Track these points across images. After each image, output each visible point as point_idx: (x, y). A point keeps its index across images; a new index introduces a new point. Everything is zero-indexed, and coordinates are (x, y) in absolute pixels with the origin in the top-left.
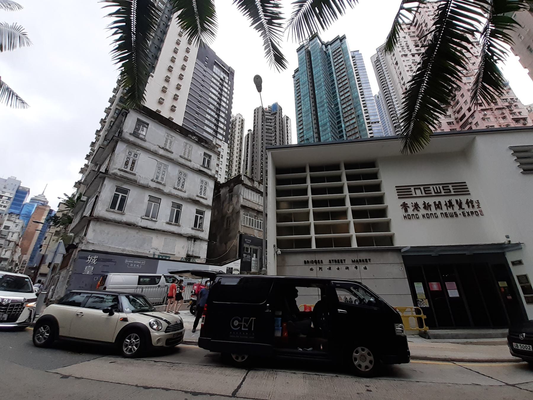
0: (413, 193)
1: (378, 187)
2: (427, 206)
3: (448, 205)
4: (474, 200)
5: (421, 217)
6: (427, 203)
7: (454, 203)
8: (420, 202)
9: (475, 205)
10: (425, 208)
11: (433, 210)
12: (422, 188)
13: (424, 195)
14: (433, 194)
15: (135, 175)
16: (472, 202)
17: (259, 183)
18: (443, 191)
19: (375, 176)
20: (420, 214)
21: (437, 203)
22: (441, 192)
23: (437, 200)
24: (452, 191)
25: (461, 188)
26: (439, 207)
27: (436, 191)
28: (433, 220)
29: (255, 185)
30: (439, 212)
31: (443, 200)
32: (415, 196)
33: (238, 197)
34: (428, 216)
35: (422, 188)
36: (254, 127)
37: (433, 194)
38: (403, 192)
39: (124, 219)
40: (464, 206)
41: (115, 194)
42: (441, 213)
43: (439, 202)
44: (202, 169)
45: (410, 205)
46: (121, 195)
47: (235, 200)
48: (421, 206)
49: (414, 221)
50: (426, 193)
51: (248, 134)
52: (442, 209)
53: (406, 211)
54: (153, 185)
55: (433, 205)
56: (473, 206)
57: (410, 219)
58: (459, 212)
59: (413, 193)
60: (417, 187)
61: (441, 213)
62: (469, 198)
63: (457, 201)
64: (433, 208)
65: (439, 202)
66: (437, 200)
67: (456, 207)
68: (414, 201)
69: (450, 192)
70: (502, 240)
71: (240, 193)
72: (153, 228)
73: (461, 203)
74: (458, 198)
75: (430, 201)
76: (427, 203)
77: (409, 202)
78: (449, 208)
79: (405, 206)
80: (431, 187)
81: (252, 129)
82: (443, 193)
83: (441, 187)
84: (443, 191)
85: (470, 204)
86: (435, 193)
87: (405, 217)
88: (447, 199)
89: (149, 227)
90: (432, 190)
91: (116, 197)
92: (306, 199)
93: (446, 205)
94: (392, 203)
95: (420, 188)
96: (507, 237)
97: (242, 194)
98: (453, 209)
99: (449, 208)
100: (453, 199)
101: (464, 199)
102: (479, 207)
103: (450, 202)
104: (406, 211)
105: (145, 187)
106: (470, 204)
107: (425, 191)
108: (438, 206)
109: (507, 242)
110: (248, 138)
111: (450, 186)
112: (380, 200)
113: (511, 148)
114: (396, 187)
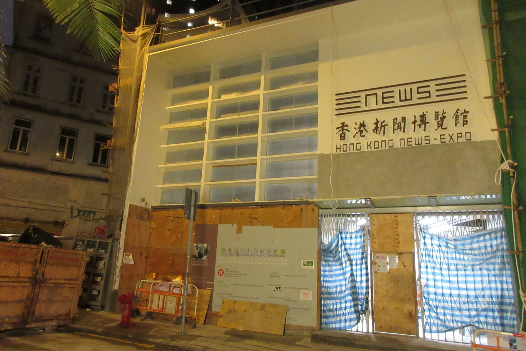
3: (418, 122)
6: (381, 120)
7: (430, 118)
8: (370, 120)
10: (376, 130)
12: (379, 92)
14: (398, 103)
15: (38, 98)
19: (314, 77)
21: (399, 120)
22: (411, 99)
23: (399, 114)
24: (434, 93)
26: (399, 127)
27: (403, 98)
31: (411, 113)
32: (366, 109)
37: (398, 103)
38: (346, 102)
39: (29, 161)
40: (449, 122)
41: (14, 128)
43: (404, 119)
44: (22, 98)
46: (22, 129)
48: (371, 126)
50: (383, 103)
52: (404, 131)
53: (343, 137)
54: (66, 109)
55: (391, 124)
56: (465, 123)
60: (370, 92)
62: (462, 105)
63: (437, 114)
65: (404, 119)
66: (399, 114)
68: (359, 118)
72: (69, 173)
73: (443, 118)
74: (439, 108)
75: (387, 117)
76: (381, 120)
78: (417, 127)
80: (396, 89)
82: (415, 101)
83: (414, 87)
84: (415, 96)
85: (461, 119)
86: (401, 101)
88: (418, 111)
89: (63, 172)
90: (397, 96)
91: (16, 134)
92: (253, 120)
93: (414, 122)
95: (376, 94)
98: (425, 130)
99: (417, 127)
100: (430, 110)
101: (450, 108)
103: (423, 117)
104: (343, 137)
105: (57, 114)
106: (461, 119)
112: (312, 120)
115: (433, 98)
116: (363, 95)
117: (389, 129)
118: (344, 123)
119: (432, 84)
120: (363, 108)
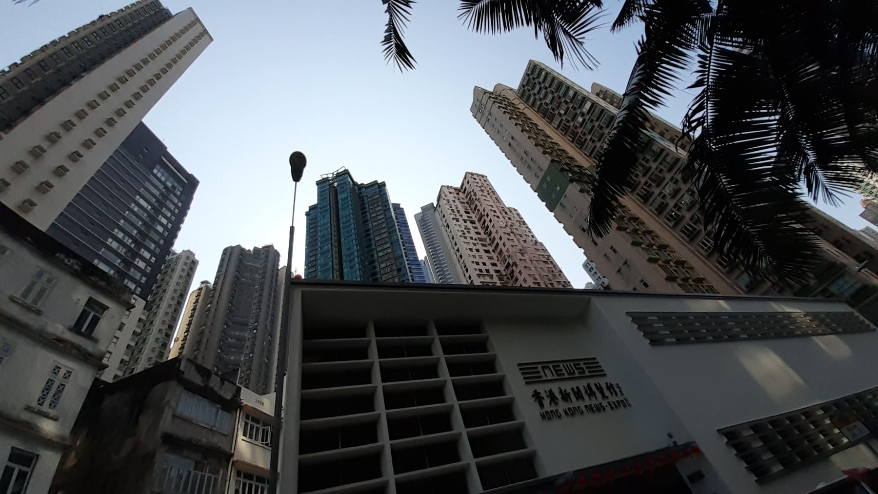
0: (542, 373)
1: (490, 365)
2: (566, 397)
4: (614, 383)
5: (563, 414)
7: (594, 389)
8: (555, 388)
9: (617, 390)
11: (575, 403)
13: (556, 377)
14: (566, 376)
16: (611, 385)
17: (223, 380)
18: (576, 372)
19: (482, 346)
20: (561, 411)
22: (574, 373)
24: (587, 371)
25: (593, 368)
28: (578, 418)
29: (212, 385)
30: (582, 404)
31: (582, 384)
33: (160, 412)
34: (572, 412)
35: (551, 366)
36: (217, 277)
37: (566, 376)
38: (530, 373)
42: (586, 406)
45: (543, 395)
47: (145, 422)
49: (555, 422)
50: (558, 375)
51: (200, 289)
53: (542, 405)
57: (550, 418)
58: (605, 403)
59: (542, 373)
60: (545, 365)
61: (586, 406)
63: (595, 384)
64: (573, 397)
65: (577, 388)
66: (574, 384)
67: (599, 395)
68: (548, 387)
69: (584, 372)
70: (663, 443)
71: (168, 403)
73: (602, 388)
75: (567, 386)
77: (542, 389)
79: (536, 395)
81: (212, 281)
84: (576, 372)
86: (568, 374)
87: (543, 416)
93: (586, 392)
94: (519, 391)
95: (548, 367)
96: (670, 436)
97: (173, 403)
100: (592, 382)
101: (602, 382)
102: (622, 394)
104: (542, 405)
107: (556, 371)
108: (579, 395)
109: (672, 444)
110: (199, 295)
111: (582, 363)
112: (498, 387)
113: (628, 313)
114: (519, 365)
115: (587, 374)
116: (540, 367)
117: (573, 397)
118: (535, 391)
119: (582, 363)
120: (544, 378)
